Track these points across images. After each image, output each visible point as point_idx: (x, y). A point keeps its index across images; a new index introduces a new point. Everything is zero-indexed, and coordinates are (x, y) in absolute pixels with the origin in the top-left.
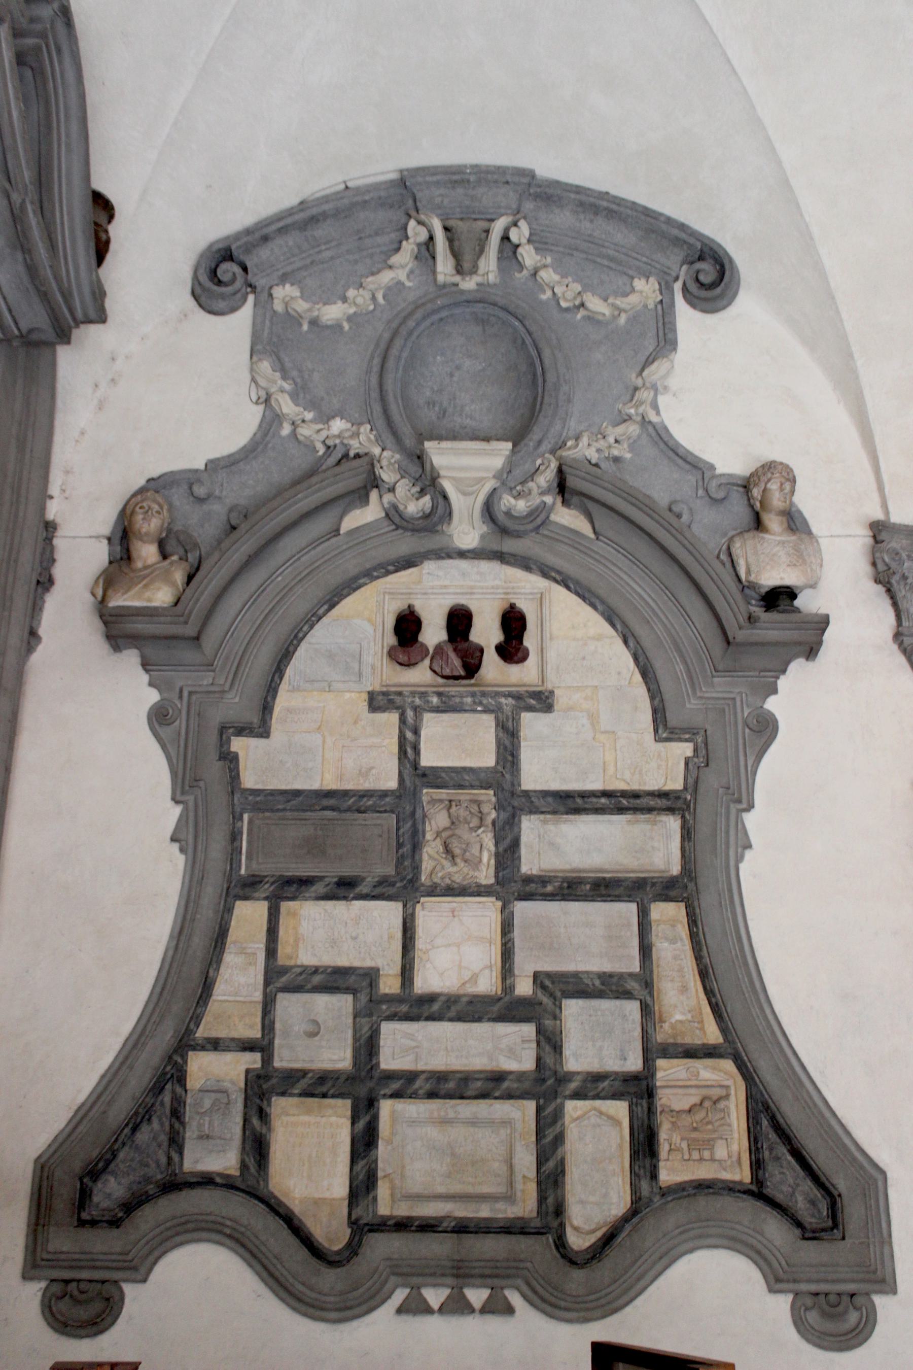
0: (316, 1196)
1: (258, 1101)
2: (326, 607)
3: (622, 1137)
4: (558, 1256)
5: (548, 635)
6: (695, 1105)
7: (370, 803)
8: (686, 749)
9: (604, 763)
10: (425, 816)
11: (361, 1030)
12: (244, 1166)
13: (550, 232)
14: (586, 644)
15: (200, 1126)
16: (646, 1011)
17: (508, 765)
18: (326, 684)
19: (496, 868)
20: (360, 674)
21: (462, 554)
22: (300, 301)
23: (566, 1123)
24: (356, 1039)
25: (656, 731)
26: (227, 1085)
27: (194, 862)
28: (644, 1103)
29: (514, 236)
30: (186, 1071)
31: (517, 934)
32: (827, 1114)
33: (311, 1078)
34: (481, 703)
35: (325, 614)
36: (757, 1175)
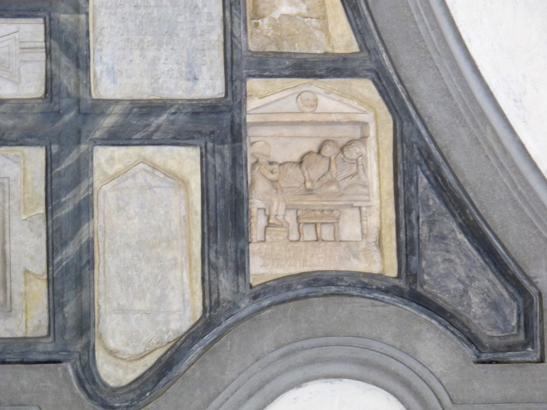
3: (189, 206)
4: (83, 396)
6: (309, 153)
23: (97, 185)
28: (226, 150)
32: (524, 168)
36: (408, 265)
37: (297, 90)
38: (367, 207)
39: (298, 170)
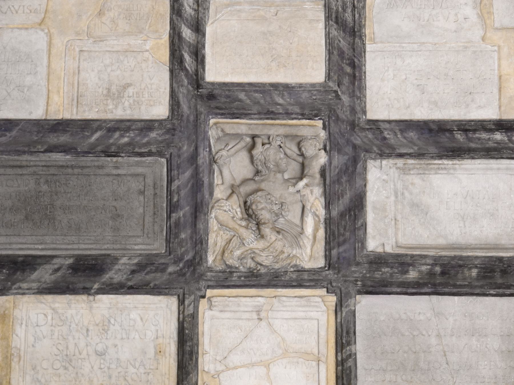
7: (126, 140)
9: (500, 77)
10: (213, 161)
17: (346, 80)
19: (327, 243)
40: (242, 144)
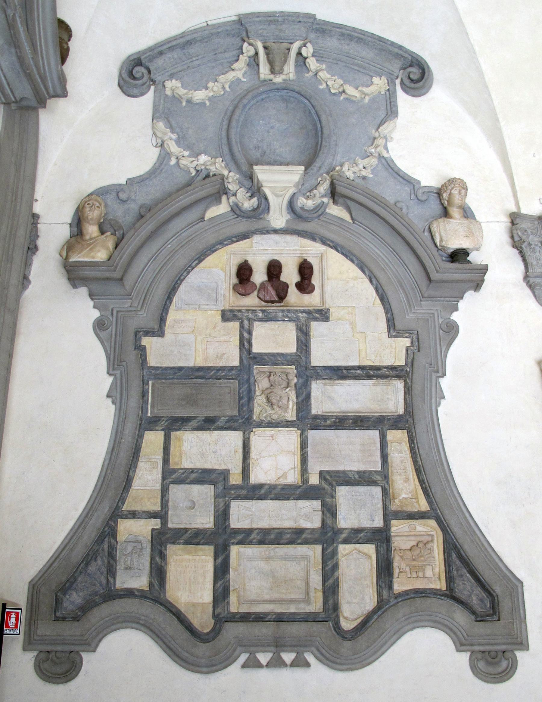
0: (195, 601)
1: (159, 547)
2: (196, 262)
3: (372, 565)
4: (335, 634)
5: (326, 278)
6: (414, 546)
8: (407, 342)
9: (359, 350)
10: (255, 381)
11: (219, 506)
12: (151, 585)
13: (324, 51)
14: (347, 283)
15: (125, 561)
16: (385, 492)
17: (304, 352)
18: (197, 306)
19: (297, 411)
20: (217, 300)
21: (276, 231)
22: (181, 89)
23: (340, 558)
24: (216, 511)
25: (389, 332)
26: (141, 538)
27: (120, 409)
28: (385, 545)
29: (304, 52)
30: (117, 530)
31: (310, 449)
32: (490, 550)
33: (190, 534)
34: (287, 316)
35: (196, 266)
36: (450, 585)
37: (409, 524)
38: (435, 565)
39: (410, 552)
40: (266, 375)
